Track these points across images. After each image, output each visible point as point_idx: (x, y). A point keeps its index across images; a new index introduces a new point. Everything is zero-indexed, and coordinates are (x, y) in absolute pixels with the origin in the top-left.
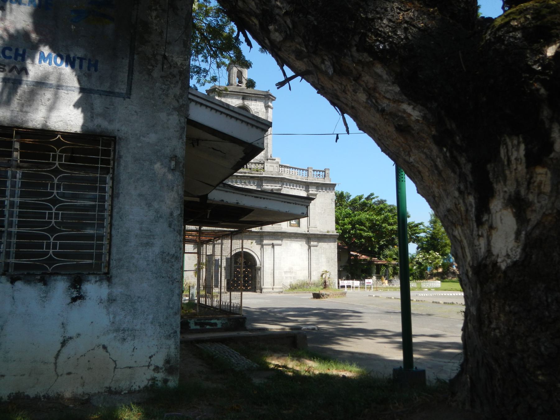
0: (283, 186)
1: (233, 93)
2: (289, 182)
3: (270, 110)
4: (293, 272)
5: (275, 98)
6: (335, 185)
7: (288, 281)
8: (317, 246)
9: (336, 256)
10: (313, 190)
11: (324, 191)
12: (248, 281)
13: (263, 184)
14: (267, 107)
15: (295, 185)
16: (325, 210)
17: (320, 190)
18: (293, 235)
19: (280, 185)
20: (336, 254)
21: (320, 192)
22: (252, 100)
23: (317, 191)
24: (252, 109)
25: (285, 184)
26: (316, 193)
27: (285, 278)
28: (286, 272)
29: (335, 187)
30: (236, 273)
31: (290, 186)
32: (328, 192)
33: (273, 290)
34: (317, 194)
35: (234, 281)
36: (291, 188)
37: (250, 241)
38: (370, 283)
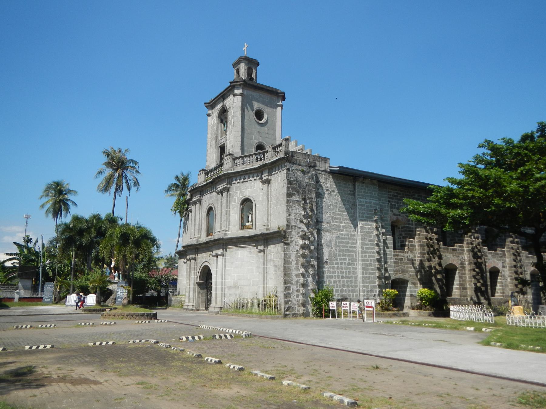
0: (233, 183)
1: (216, 99)
2: (239, 175)
4: (238, 288)
7: (230, 300)
9: (282, 263)
11: (277, 172)
15: (247, 176)
16: (278, 198)
18: (235, 240)
19: (226, 183)
20: (282, 261)
21: (274, 174)
22: (227, 97)
23: (271, 175)
24: (227, 107)
25: (234, 179)
26: (267, 177)
27: (228, 295)
28: (230, 288)
31: (240, 179)
32: (280, 172)
36: (243, 182)
37: (209, 253)
38: (371, 307)
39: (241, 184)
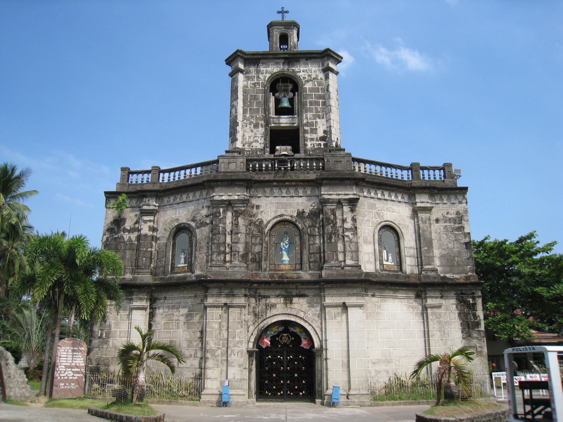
3: (331, 75)
5: (342, 58)
6: (466, 189)
8: (439, 307)
10: (424, 200)
12: (299, 380)
13: (322, 193)
14: (327, 70)
17: (437, 202)
21: (438, 204)
26: (428, 205)
29: (466, 193)
30: (276, 364)
32: (454, 204)
33: (348, 398)
34: (433, 207)
35: (271, 380)
39: (377, 202)
